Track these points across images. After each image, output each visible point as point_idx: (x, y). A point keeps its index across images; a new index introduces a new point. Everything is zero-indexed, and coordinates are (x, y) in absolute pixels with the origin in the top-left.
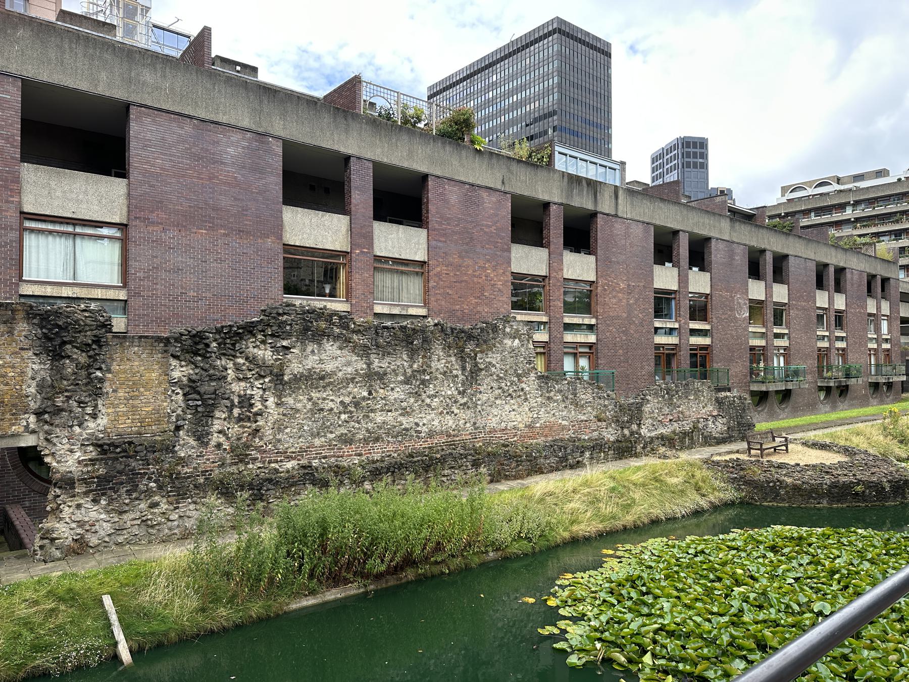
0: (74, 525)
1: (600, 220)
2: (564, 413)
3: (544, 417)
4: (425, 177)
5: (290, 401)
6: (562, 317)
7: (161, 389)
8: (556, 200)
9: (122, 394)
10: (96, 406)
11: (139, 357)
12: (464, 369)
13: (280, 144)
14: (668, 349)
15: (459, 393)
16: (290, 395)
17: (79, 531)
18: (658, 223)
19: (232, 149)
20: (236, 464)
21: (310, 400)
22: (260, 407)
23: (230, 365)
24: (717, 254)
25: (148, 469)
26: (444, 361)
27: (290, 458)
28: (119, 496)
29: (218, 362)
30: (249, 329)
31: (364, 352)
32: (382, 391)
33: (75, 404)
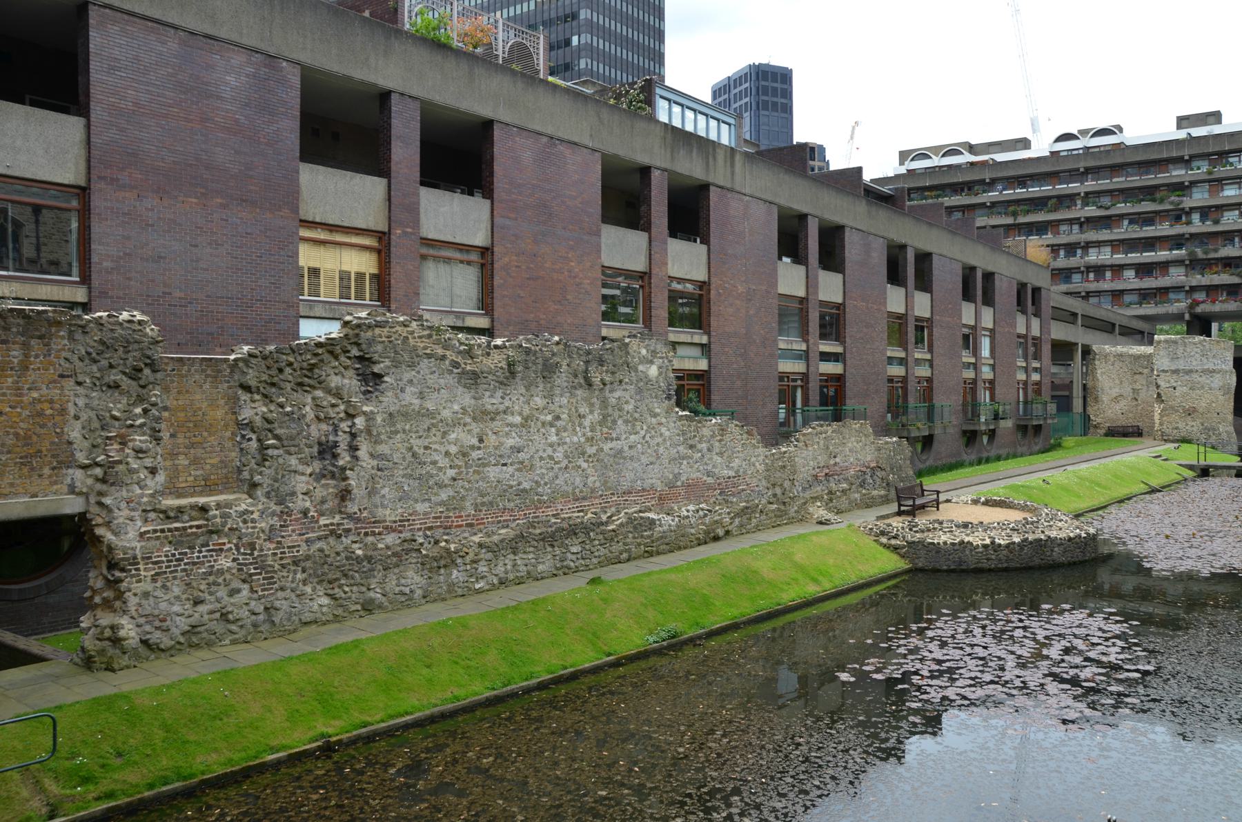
0: (142, 620)
1: (714, 193)
4: (488, 125)
6: (667, 333)
7: (228, 434)
8: (658, 164)
11: (201, 387)
13: (297, 71)
17: (148, 628)
18: (783, 202)
19: (232, 77)
22: (348, 459)
23: (309, 399)
24: (852, 248)
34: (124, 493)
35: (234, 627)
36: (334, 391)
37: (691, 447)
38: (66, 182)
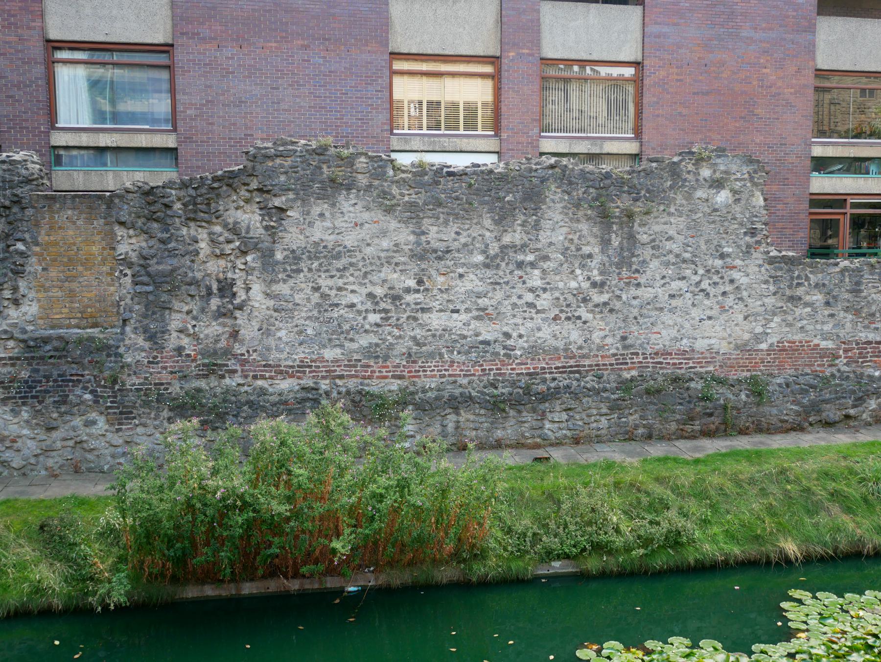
2: (827, 328)
3: (777, 332)
5: (283, 289)
7: (106, 269)
9: (54, 274)
10: (15, 289)
11: (74, 223)
12: (605, 243)
14: (855, 206)
15: (594, 285)
16: (285, 281)
20: (206, 376)
21: (317, 289)
23: (203, 235)
25: (82, 376)
26: (565, 230)
27: (284, 374)
28: (46, 408)
29: (184, 231)
30: (230, 180)
31: (413, 214)
32: (441, 279)
35: (89, 456)
36: (231, 226)
37: (792, 299)
38: (156, 41)
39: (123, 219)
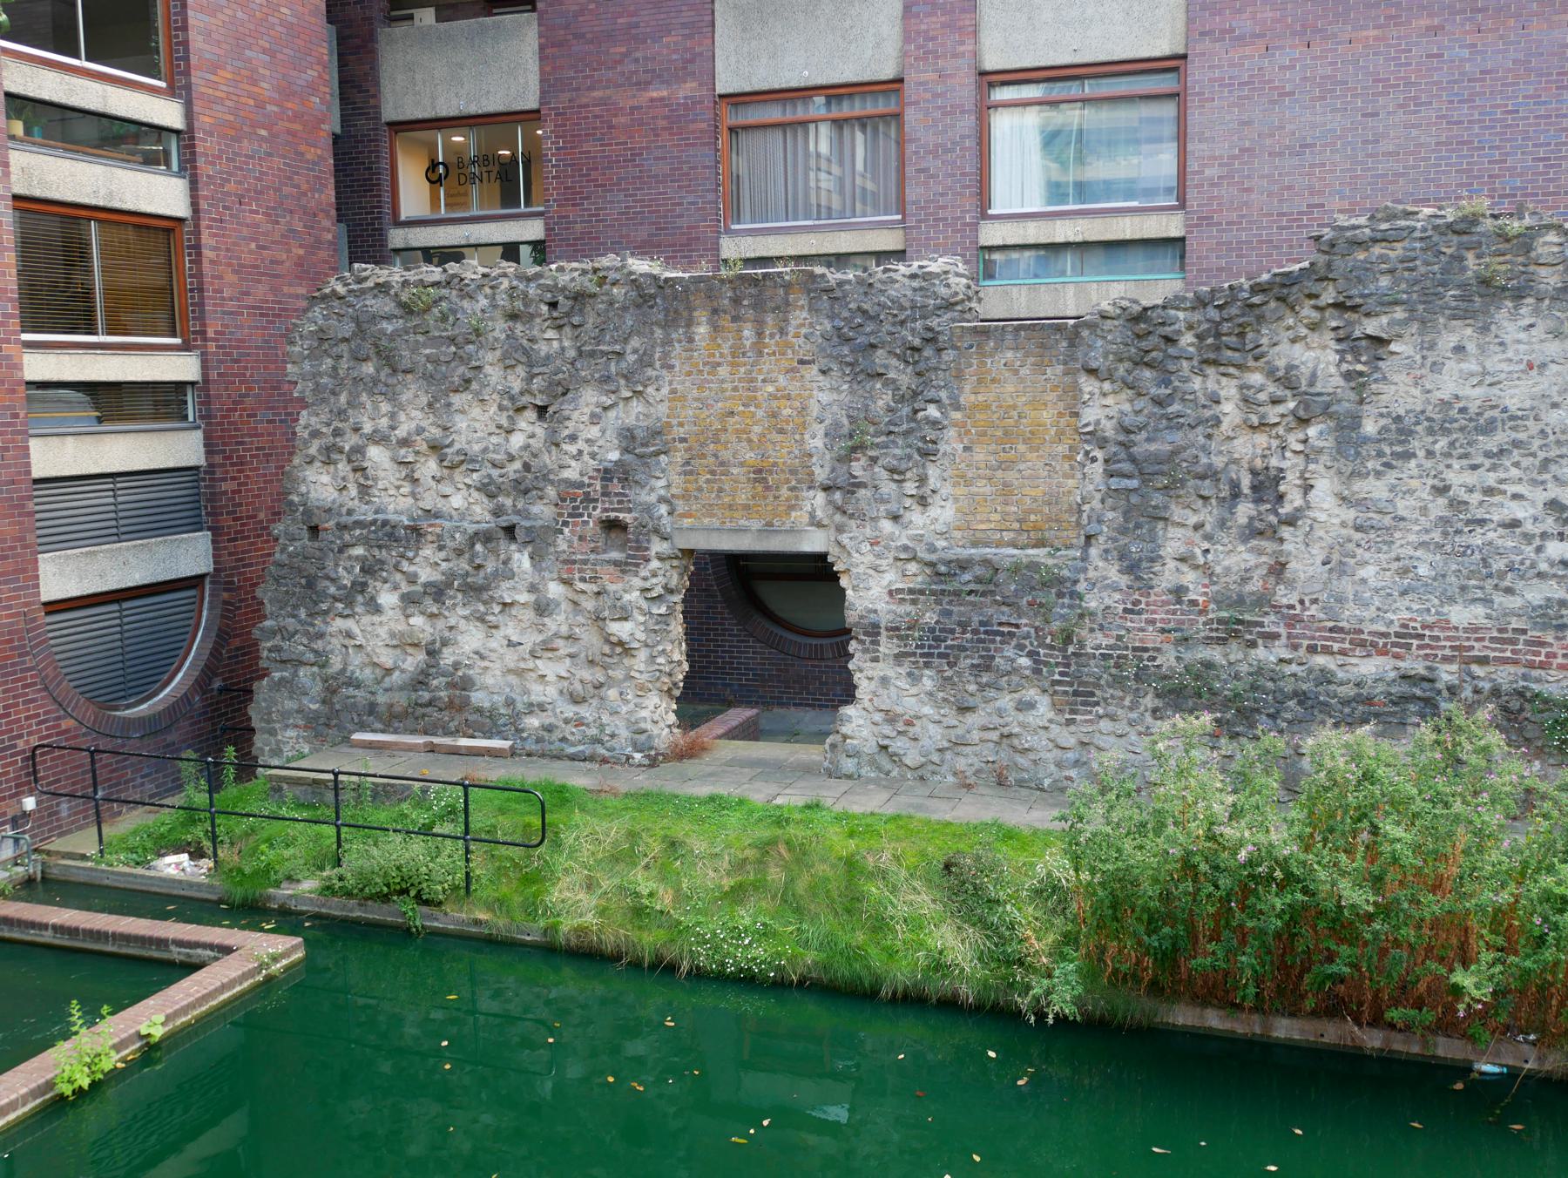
0: (878, 717)
5: (1375, 489)
7: (1062, 449)
9: (981, 457)
10: (922, 480)
11: (1016, 372)
20: (1222, 641)
21: (1441, 490)
25: (1017, 626)
28: (959, 674)
29: (1197, 384)
30: (1283, 290)
33: (884, 474)
34: (868, 531)
35: (1022, 761)
36: (1281, 373)
38: (1157, 53)
39: (1094, 365)
